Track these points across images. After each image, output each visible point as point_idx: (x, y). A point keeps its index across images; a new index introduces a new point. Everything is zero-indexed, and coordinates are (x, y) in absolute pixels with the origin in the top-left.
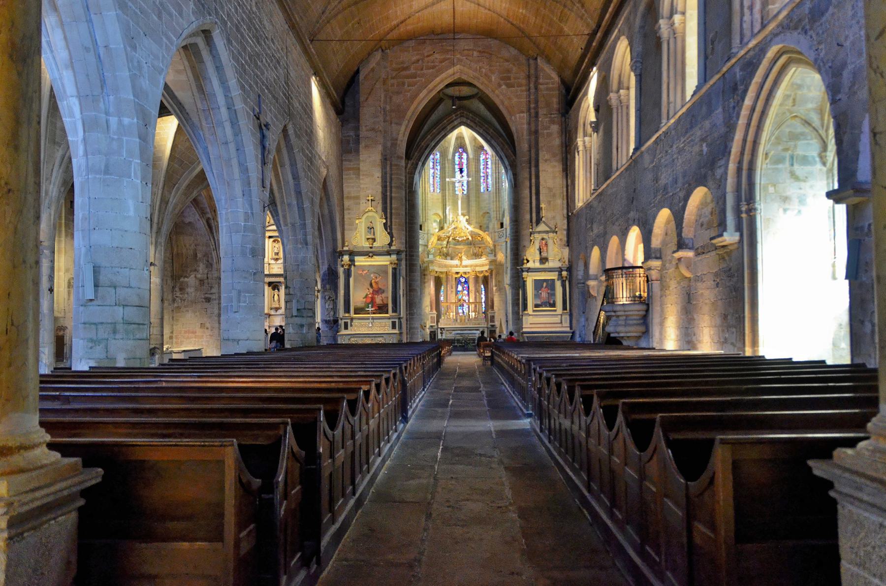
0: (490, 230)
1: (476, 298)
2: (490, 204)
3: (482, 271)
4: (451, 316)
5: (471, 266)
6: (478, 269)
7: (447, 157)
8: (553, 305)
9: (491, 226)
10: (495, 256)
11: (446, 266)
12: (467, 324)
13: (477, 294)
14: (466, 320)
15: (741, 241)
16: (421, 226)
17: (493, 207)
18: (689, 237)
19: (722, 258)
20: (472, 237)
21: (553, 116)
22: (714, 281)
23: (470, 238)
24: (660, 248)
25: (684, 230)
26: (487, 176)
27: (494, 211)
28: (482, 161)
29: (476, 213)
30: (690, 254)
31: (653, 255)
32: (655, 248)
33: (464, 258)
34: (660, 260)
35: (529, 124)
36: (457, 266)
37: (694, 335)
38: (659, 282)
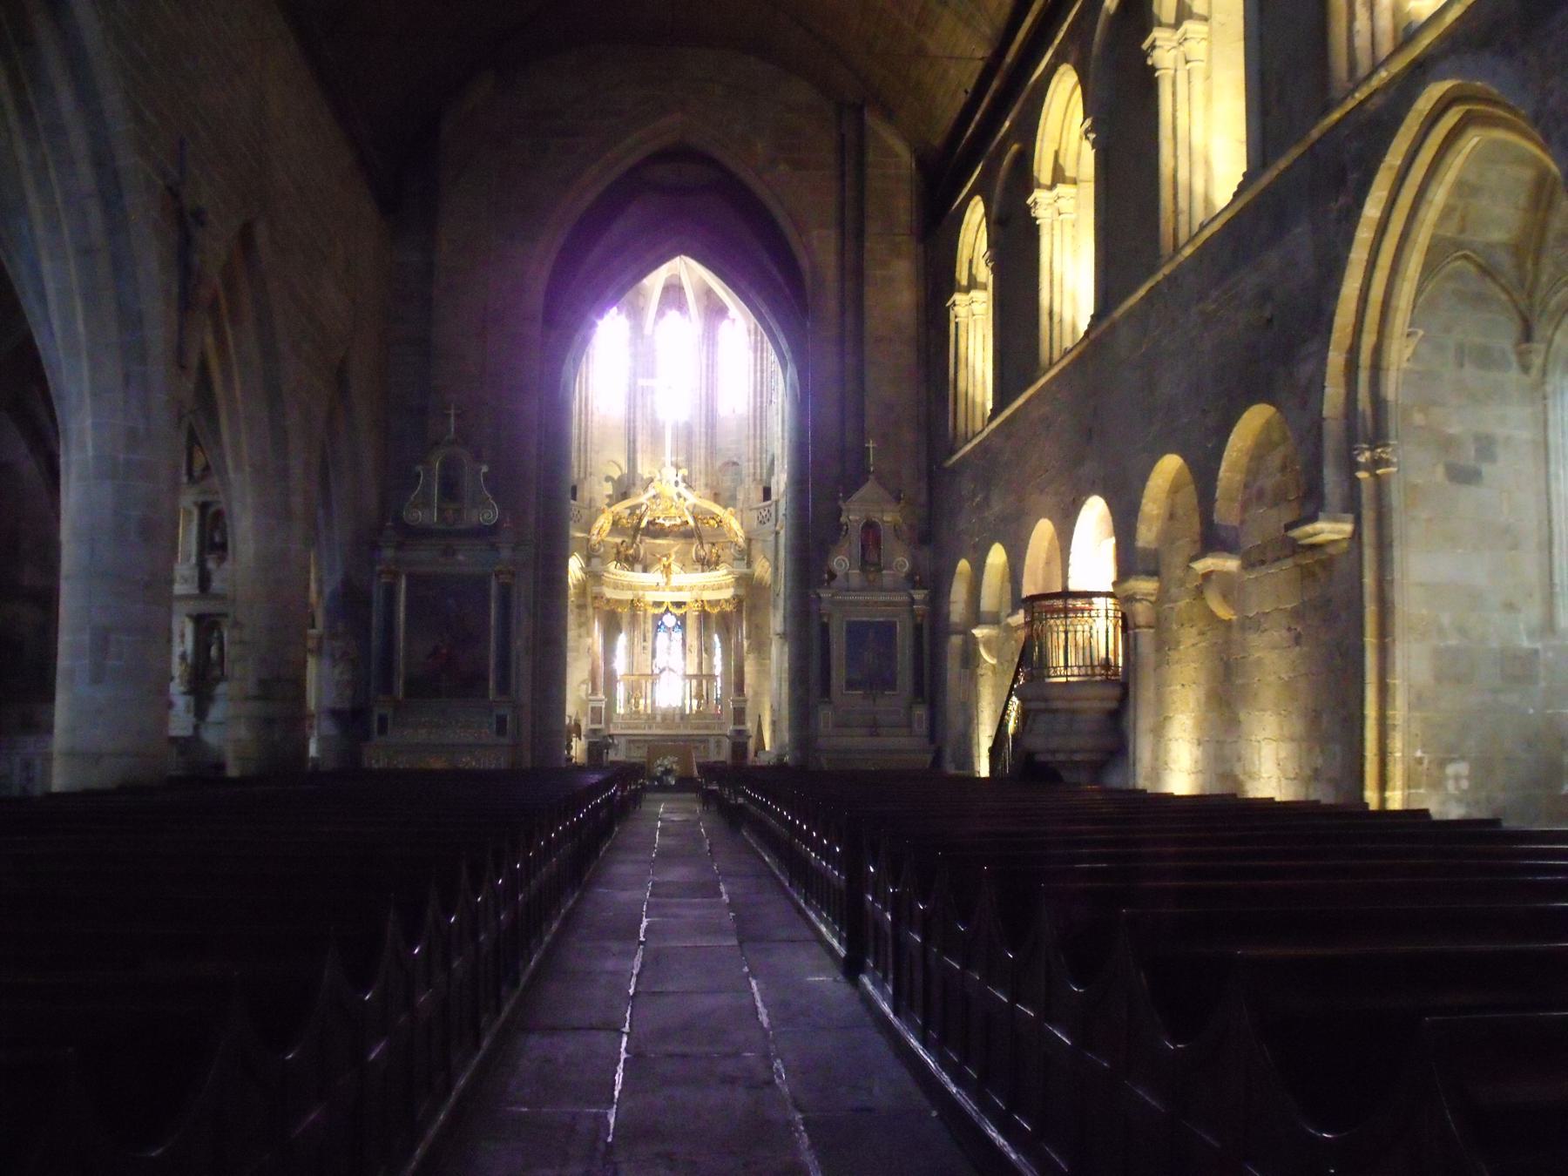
0: (740, 505)
1: (700, 664)
3: (719, 601)
4: (641, 707)
5: (692, 589)
6: (708, 596)
8: (889, 683)
9: (741, 496)
10: (749, 564)
11: (630, 587)
13: (704, 655)
15: (1357, 535)
16: (574, 490)
18: (1229, 523)
19: (1307, 574)
20: (695, 519)
21: (898, 239)
22: (1289, 629)
23: (691, 523)
24: (1156, 549)
25: (1218, 505)
27: (749, 460)
29: (707, 464)
30: (1231, 564)
31: (1140, 568)
32: (1145, 549)
33: (675, 567)
34: (1156, 578)
35: (841, 254)
36: (657, 587)
37: (1239, 759)
38: (1152, 631)
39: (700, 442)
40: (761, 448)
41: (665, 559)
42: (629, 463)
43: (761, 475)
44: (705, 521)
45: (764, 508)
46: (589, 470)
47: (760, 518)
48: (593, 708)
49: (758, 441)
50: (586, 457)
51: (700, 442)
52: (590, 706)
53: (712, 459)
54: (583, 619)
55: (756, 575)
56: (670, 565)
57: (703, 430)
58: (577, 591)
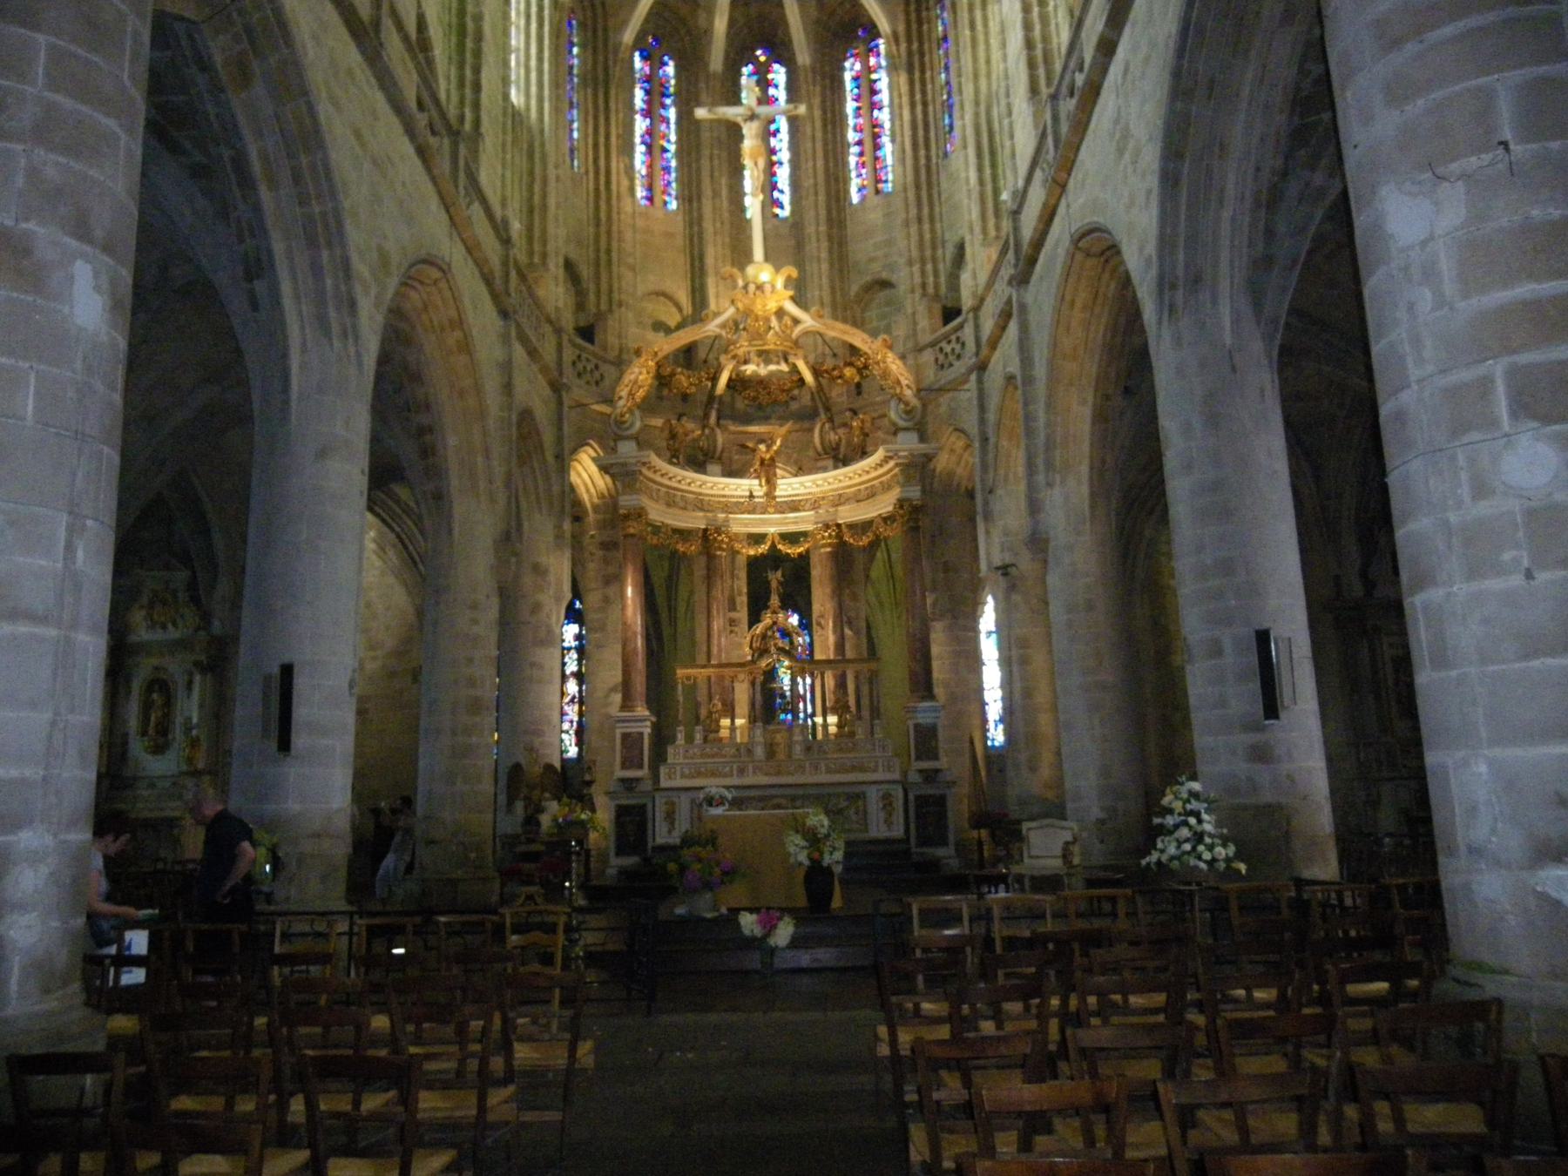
1: (840, 646)
2: (889, 242)
4: (724, 733)
5: (815, 504)
6: (849, 514)
7: (707, 65)
11: (700, 504)
12: (801, 769)
13: (847, 632)
14: (798, 749)
17: (904, 243)
20: (816, 373)
23: (808, 377)
26: (876, 136)
28: (849, 84)
29: (833, 289)
36: (749, 504)
39: (819, 248)
40: (933, 240)
41: (762, 447)
42: (693, 298)
44: (836, 373)
46: (616, 296)
47: (941, 357)
48: (625, 736)
49: (926, 227)
50: (610, 272)
51: (819, 248)
52: (618, 732)
53: (842, 281)
54: (611, 570)
55: (938, 470)
57: (823, 228)
58: (600, 517)
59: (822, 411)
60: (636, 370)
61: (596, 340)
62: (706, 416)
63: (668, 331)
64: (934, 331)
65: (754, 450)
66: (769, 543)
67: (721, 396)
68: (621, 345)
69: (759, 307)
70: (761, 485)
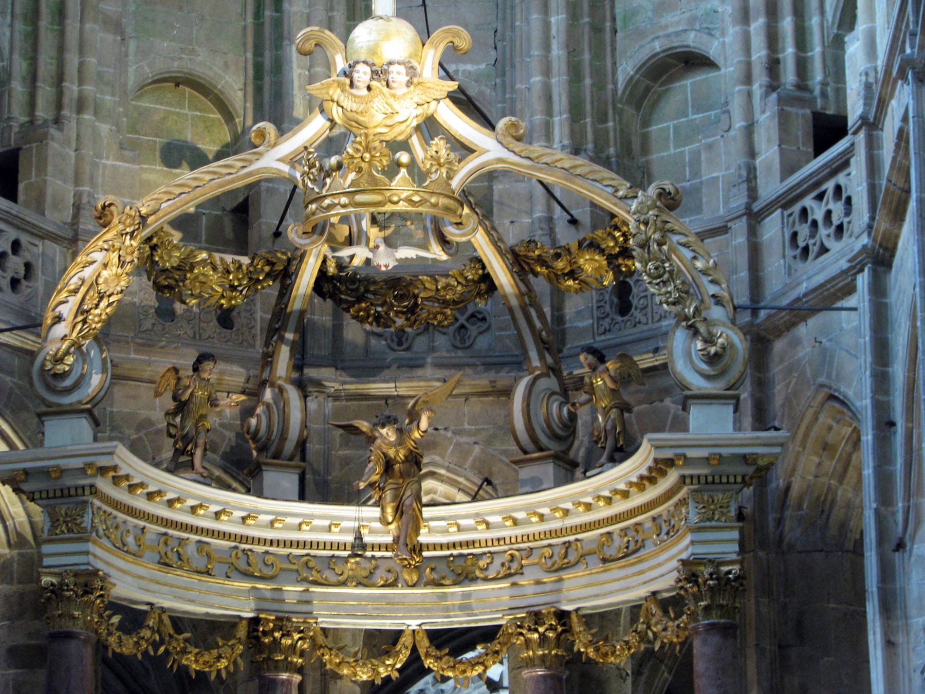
29: (575, 72)
41: (388, 433)
43: (802, 66)
44: (560, 264)
45: (814, 186)
46: (72, 88)
47: (804, 230)
50: (62, 33)
53: (598, 53)
56: (414, 460)
59: (533, 354)
60: (98, 256)
61: (21, 187)
62: (268, 360)
63: (198, 159)
64: (788, 169)
65: (371, 439)
66: (404, 656)
67: (302, 313)
68: (78, 195)
69: (379, 118)
70: (383, 520)
